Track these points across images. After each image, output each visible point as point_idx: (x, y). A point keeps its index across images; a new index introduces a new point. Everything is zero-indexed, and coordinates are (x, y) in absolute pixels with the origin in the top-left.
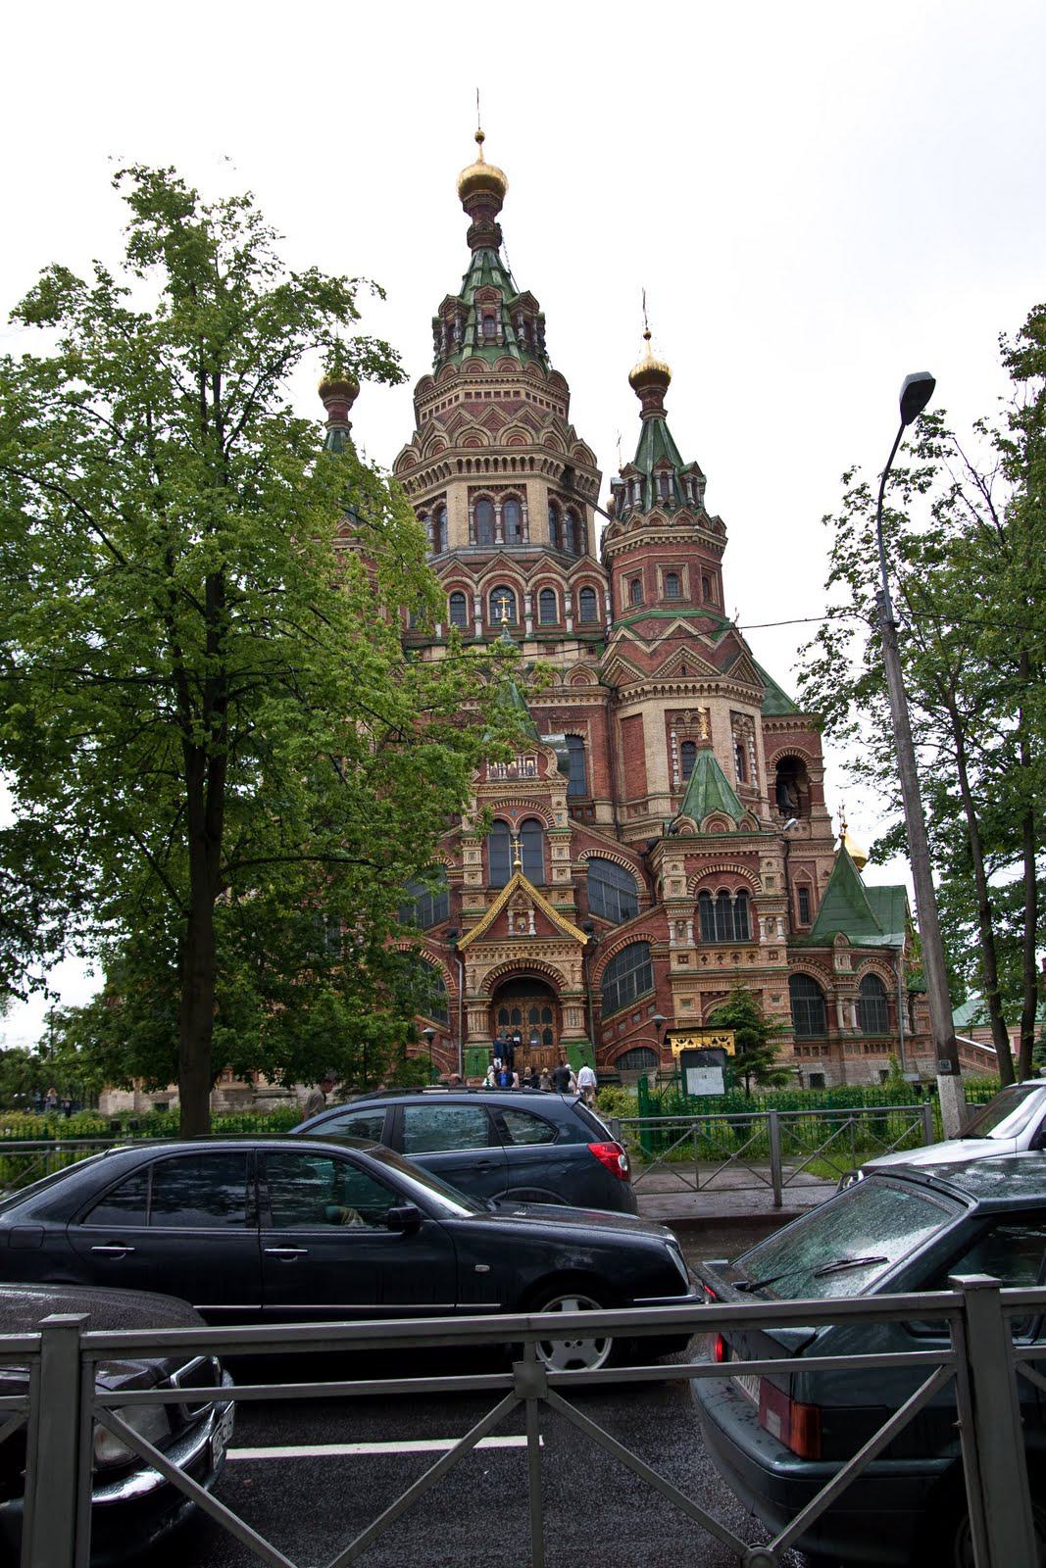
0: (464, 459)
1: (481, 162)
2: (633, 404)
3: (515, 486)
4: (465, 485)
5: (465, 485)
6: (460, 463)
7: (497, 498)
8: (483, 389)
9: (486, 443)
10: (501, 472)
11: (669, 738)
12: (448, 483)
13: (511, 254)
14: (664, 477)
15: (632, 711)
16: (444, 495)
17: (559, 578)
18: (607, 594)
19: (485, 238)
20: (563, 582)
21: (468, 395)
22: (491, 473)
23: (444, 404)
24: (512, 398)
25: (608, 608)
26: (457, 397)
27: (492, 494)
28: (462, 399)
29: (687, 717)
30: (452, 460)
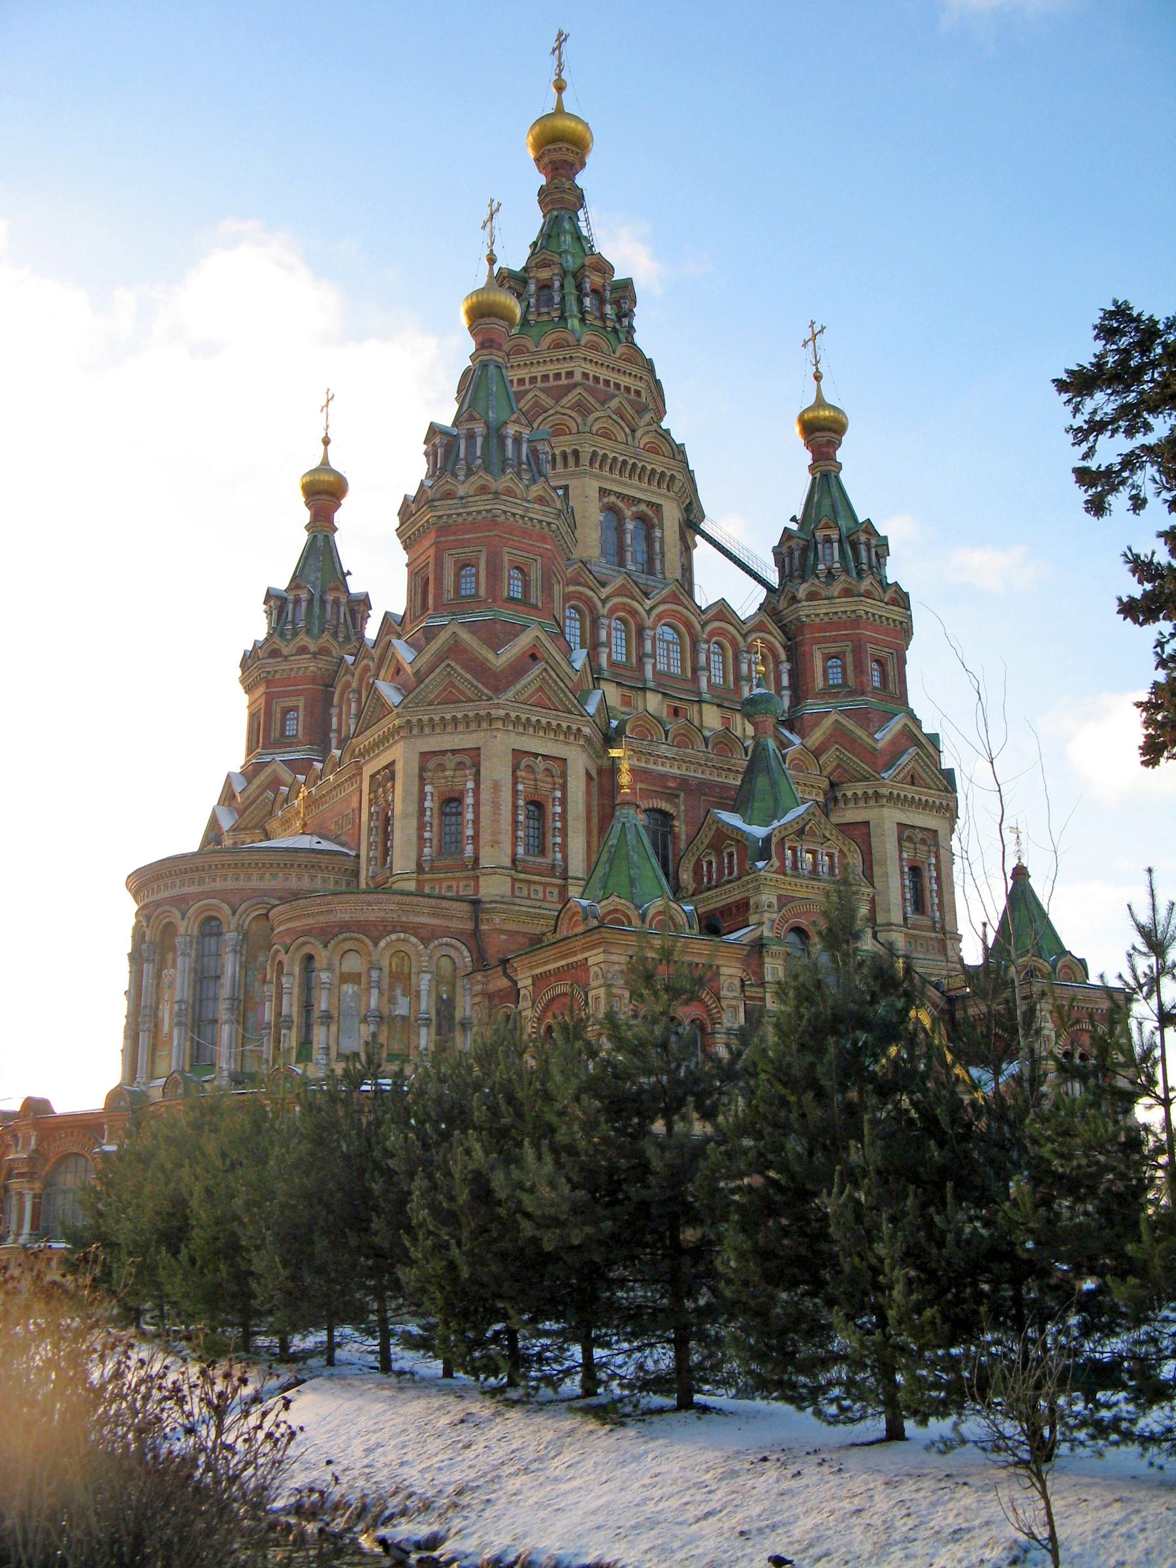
0: (601, 453)
1: (560, 111)
3: (649, 503)
4: (596, 484)
5: (596, 484)
6: (595, 453)
7: (628, 513)
8: (604, 374)
10: (635, 482)
11: (901, 859)
12: (573, 475)
15: (851, 815)
17: (735, 632)
18: (785, 667)
20: (740, 638)
21: (585, 376)
25: (785, 681)
26: (570, 374)
27: (621, 505)
28: (578, 377)
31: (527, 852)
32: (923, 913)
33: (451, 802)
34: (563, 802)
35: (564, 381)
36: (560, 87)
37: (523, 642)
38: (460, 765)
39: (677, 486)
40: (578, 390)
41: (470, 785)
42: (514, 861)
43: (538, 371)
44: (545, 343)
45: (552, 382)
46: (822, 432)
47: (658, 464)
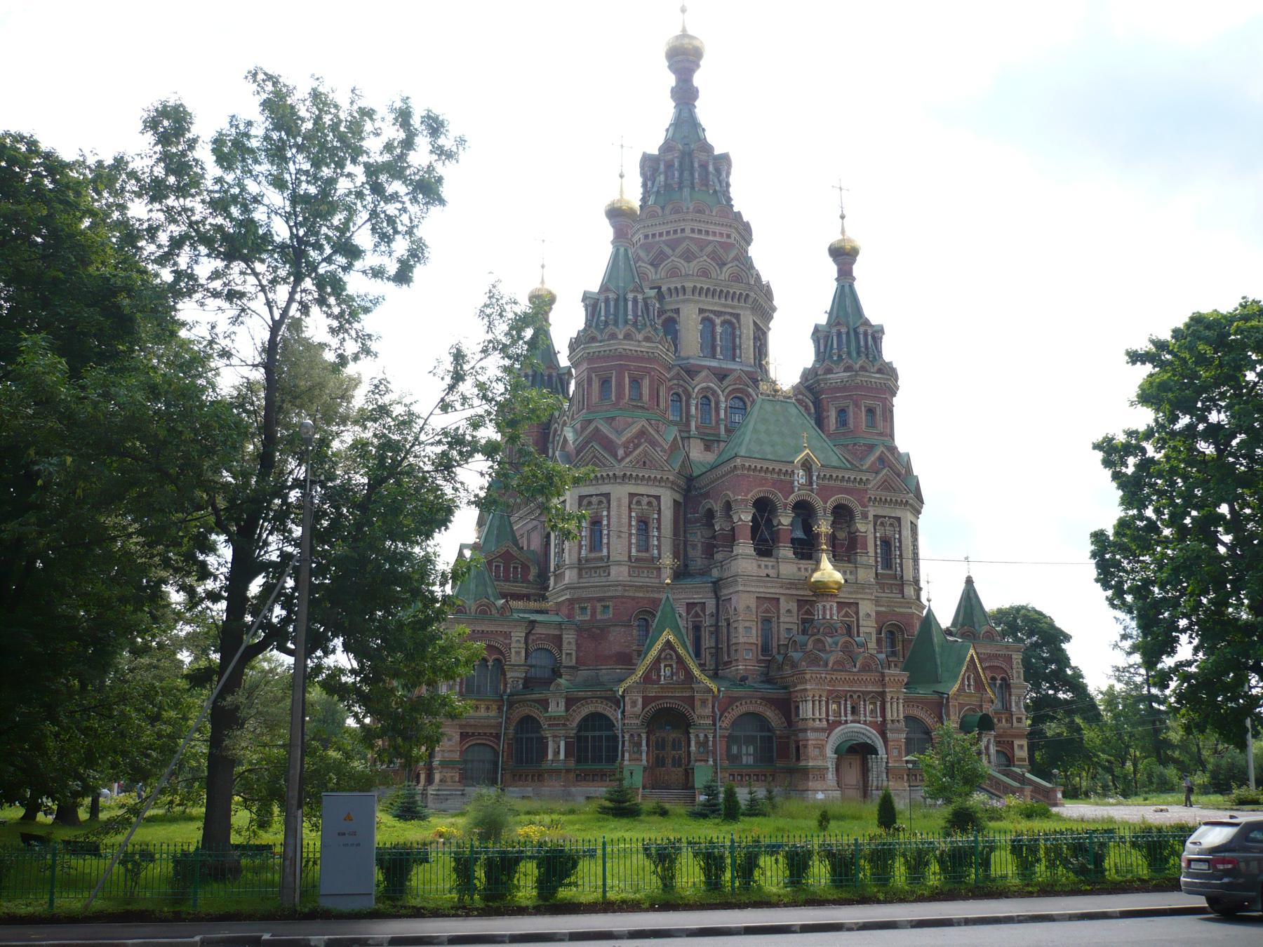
2: (832, 269)
3: (731, 314)
7: (718, 321)
8: (703, 227)
9: (714, 276)
12: (684, 301)
13: (703, 111)
14: (866, 334)
16: (677, 311)
19: (685, 95)
22: (716, 300)
23: (668, 233)
26: (683, 230)
28: (688, 231)
30: (689, 285)
31: (638, 551)
32: (891, 568)
34: (659, 520)
35: (679, 235)
37: (635, 429)
38: (600, 502)
39: (750, 300)
40: (687, 242)
41: (605, 513)
42: (630, 557)
43: (664, 229)
44: (667, 211)
45: (672, 237)
46: (844, 256)
47: (737, 289)
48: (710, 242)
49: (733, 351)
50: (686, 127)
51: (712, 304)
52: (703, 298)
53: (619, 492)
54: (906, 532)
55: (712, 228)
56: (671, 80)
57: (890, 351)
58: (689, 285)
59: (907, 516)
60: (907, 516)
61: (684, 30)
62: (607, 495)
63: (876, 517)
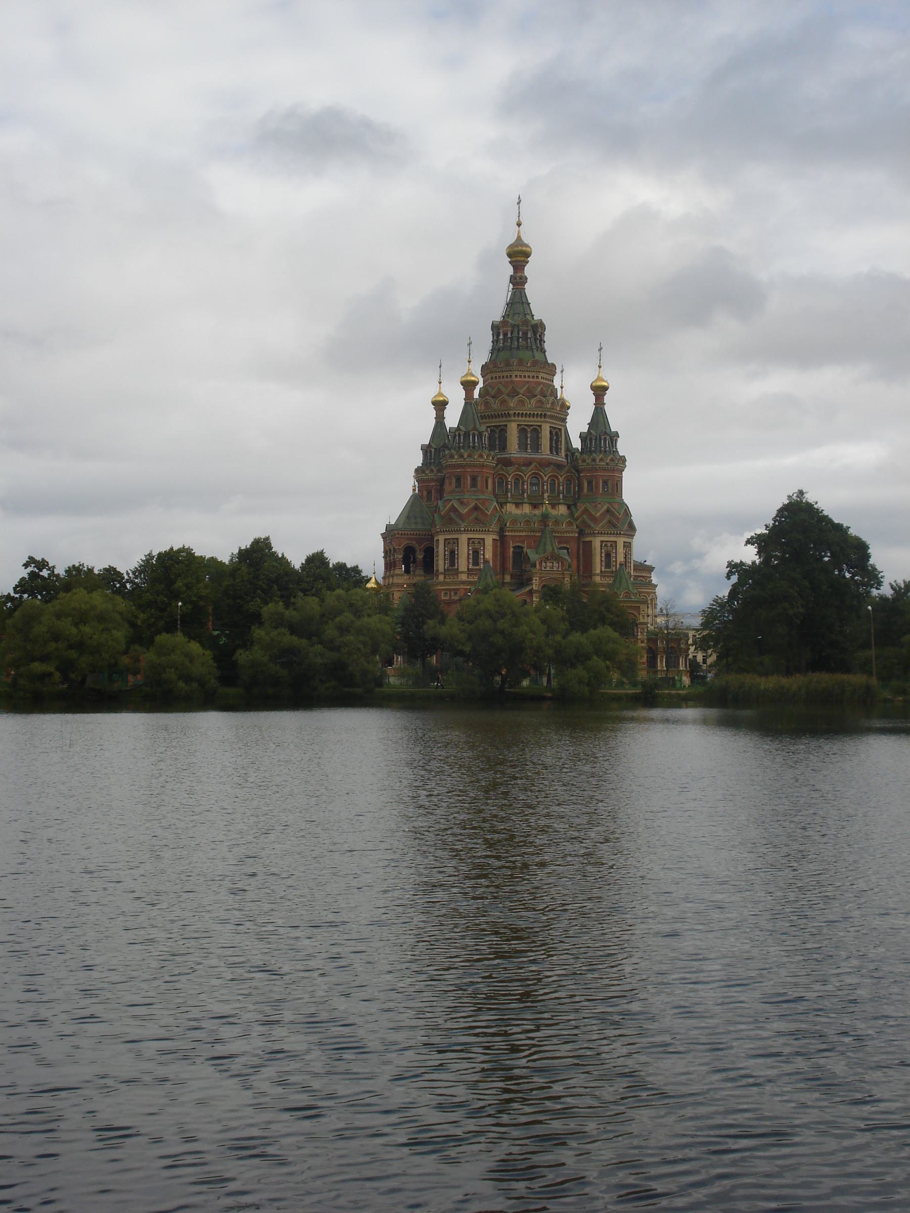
13: (530, 289)
19: (518, 281)
24: (535, 380)
26: (511, 376)
28: (513, 376)
29: (609, 544)
33: (452, 553)
34: (484, 550)
36: (519, 225)
43: (501, 374)
48: (528, 382)
49: (537, 447)
50: (518, 301)
51: (525, 421)
52: (520, 418)
53: (463, 538)
54: (621, 549)
55: (527, 374)
56: (510, 270)
57: (622, 448)
58: (511, 412)
59: (621, 541)
60: (621, 541)
61: (519, 238)
62: (457, 539)
63: (602, 542)
